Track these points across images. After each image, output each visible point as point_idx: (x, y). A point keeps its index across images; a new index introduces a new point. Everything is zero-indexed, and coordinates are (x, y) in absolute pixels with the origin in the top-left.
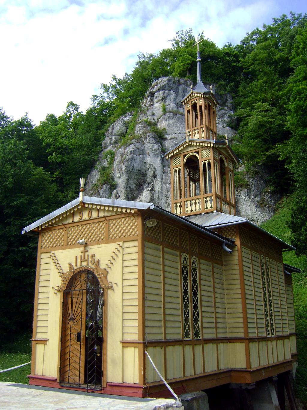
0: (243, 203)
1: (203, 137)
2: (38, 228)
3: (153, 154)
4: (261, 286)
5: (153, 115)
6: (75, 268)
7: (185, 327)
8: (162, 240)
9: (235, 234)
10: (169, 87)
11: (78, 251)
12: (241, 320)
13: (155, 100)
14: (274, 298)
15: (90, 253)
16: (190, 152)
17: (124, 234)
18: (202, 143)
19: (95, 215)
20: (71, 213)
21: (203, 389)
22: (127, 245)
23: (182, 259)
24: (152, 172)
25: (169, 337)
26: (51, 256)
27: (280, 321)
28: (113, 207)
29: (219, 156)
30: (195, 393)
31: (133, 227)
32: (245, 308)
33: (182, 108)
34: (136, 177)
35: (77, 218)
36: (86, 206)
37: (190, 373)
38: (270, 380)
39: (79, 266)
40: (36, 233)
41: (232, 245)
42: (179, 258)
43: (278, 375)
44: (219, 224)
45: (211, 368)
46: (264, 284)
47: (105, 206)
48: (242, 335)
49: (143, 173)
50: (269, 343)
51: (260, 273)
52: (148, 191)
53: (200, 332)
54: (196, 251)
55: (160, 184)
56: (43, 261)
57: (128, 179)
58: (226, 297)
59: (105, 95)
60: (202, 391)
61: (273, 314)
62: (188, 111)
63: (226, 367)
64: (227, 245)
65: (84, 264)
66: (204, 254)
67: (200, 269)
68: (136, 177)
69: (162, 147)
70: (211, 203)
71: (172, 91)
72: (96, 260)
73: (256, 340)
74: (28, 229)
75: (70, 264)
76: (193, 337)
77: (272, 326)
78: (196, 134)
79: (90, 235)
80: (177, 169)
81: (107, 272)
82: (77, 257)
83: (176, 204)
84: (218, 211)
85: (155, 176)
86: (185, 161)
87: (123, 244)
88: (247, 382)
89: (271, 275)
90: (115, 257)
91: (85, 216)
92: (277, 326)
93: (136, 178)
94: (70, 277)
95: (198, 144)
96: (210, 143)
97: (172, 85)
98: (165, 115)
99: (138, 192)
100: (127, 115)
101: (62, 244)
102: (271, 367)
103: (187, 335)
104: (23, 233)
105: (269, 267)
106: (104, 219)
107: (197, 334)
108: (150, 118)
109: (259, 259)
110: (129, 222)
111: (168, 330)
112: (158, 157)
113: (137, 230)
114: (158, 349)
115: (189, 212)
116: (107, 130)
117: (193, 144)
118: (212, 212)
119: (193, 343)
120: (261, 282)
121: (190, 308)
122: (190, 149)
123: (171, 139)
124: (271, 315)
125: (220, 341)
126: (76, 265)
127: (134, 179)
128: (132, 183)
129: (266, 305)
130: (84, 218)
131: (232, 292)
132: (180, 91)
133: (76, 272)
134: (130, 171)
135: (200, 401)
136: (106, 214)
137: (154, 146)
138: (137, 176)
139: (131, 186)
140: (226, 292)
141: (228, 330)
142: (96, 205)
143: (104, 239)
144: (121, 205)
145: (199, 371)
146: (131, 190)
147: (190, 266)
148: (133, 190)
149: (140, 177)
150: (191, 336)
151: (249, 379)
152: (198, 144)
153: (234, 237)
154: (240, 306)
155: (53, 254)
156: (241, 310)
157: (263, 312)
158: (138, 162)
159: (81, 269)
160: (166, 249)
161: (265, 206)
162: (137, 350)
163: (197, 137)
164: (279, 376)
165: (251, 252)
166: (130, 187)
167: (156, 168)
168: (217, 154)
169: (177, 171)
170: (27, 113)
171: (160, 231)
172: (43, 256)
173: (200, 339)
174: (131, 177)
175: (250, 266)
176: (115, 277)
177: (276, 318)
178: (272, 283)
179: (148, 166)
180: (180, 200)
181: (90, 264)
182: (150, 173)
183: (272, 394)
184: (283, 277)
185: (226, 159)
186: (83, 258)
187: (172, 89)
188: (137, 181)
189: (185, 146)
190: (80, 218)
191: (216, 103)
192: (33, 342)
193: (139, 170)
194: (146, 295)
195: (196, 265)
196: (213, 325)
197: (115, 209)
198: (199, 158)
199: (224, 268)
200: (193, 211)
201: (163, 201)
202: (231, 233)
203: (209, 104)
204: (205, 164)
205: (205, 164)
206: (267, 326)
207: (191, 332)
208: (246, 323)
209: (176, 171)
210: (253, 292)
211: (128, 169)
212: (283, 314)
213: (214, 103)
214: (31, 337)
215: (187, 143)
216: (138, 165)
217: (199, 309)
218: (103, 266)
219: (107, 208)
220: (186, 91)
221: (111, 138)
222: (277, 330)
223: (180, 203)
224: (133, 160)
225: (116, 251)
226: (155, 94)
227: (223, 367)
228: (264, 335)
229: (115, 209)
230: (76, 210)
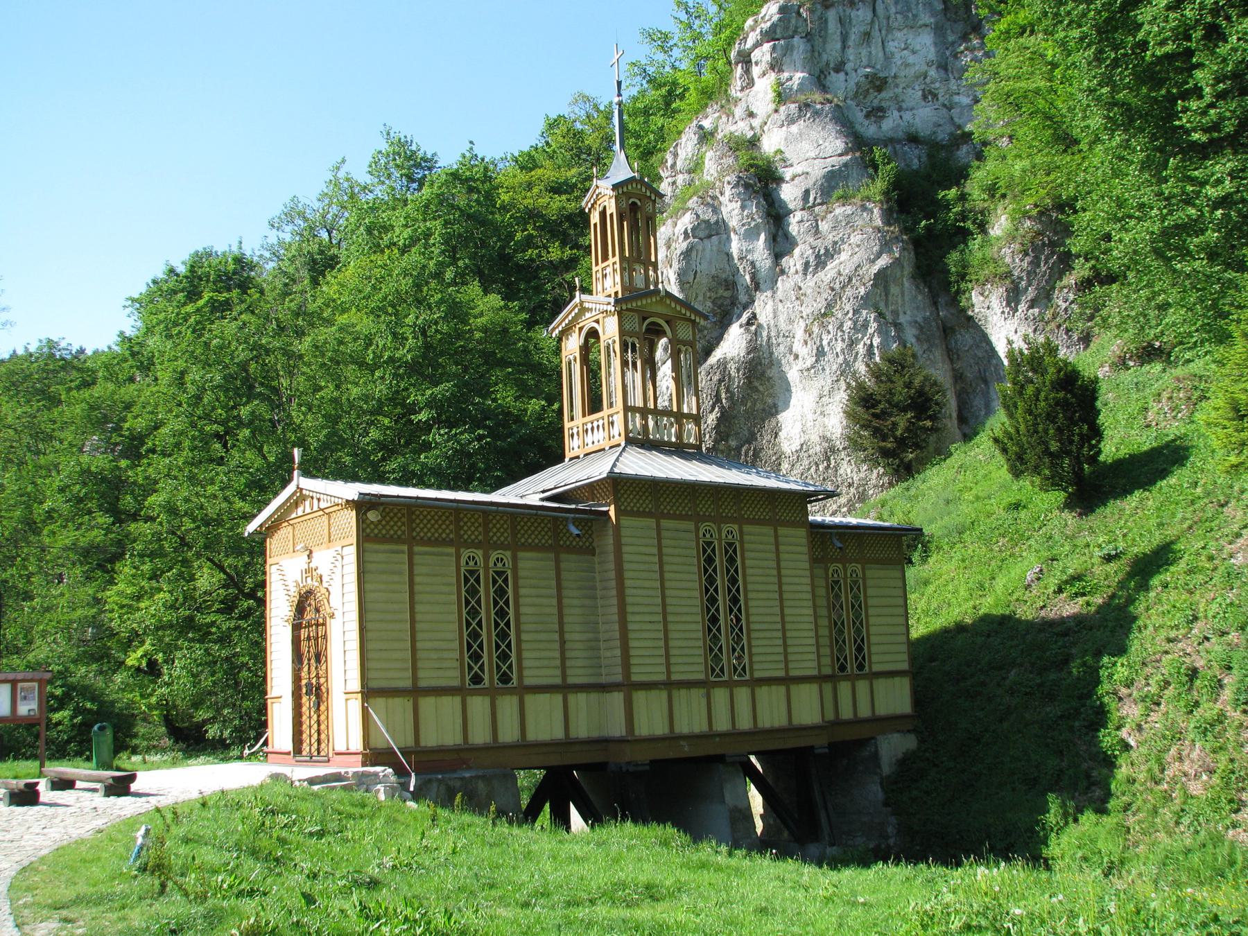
2: (261, 526)
5: (751, 115)
10: (786, 28)
13: (756, 71)
16: (587, 322)
33: (842, 76)
38: (720, 759)
48: (619, 678)
52: (741, 326)
59: (660, 57)
64: (575, 521)
67: (515, 569)
71: (796, 39)
74: (252, 527)
86: (582, 340)
97: (793, 21)
98: (776, 111)
100: (709, 110)
103: (477, 679)
107: (505, 679)
108: (741, 124)
116: (663, 162)
119: (492, 693)
122: (588, 315)
123: (793, 180)
132: (833, 26)
141: (603, 671)
161: (1059, 327)
170: (471, 142)
171: (403, 524)
176: (335, 600)
185: (667, 322)
187: (795, 32)
188: (713, 302)
192: (269, 701)
199: (596, 559)
201: (782, 348)
203: (634, 204)
207: (486, 677)
214: (266, 694)
221: (674, 183)
224: (694, 254)
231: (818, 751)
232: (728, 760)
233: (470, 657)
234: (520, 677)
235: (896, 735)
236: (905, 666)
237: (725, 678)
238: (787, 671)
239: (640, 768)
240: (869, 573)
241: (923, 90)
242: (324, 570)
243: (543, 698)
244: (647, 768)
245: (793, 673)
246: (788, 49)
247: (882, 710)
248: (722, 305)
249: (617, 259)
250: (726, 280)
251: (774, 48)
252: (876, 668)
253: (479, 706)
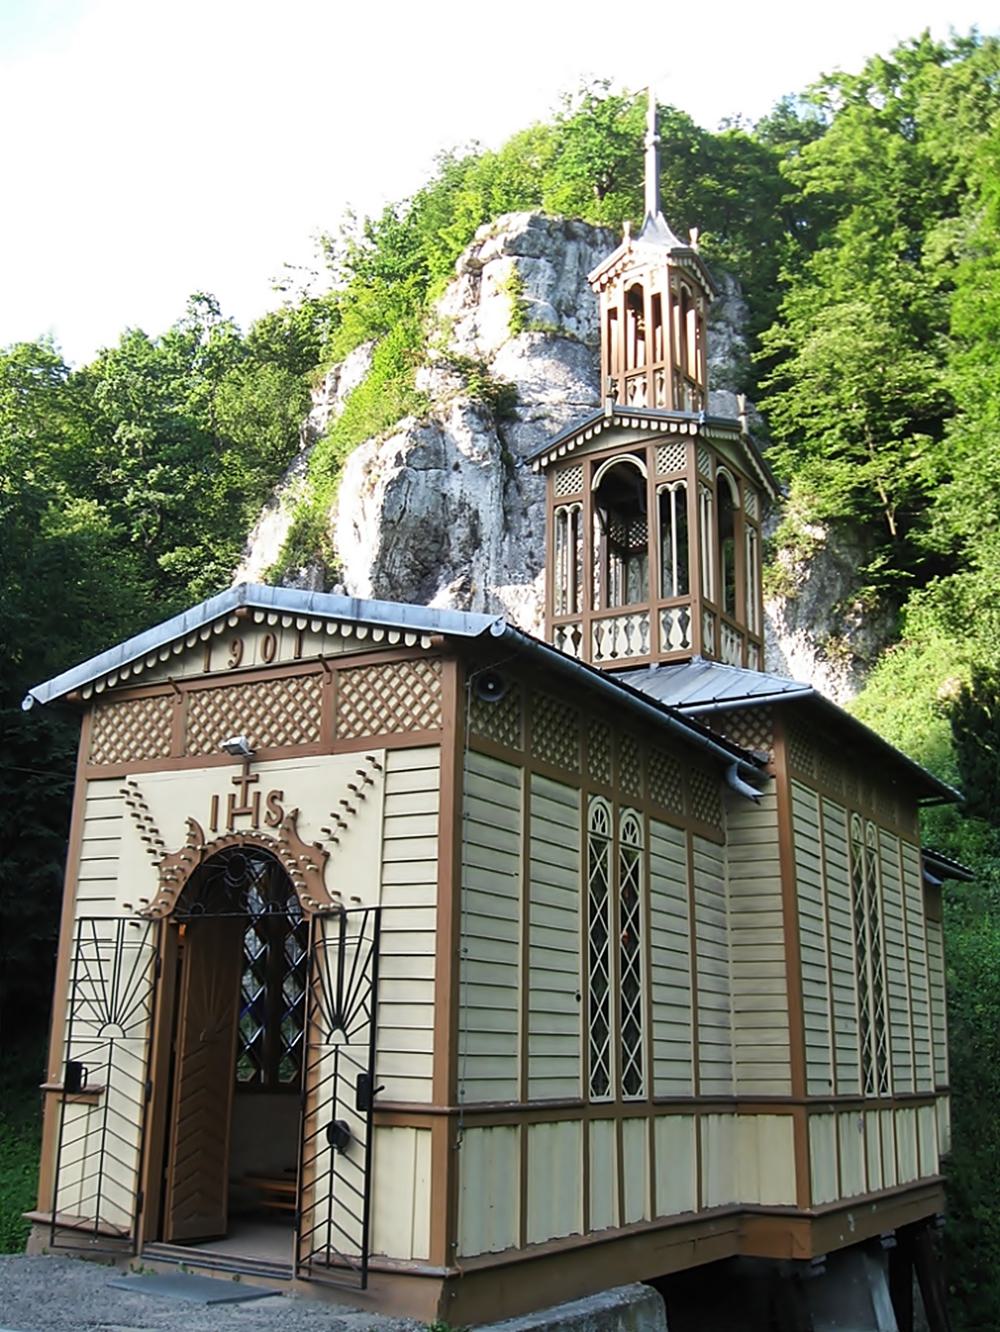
0: (770, 643)
1: (661, 404)
2: (81, 689)
3: (471, 467)
4: (850, 921)
6: (210, 837)
7: (595, 1058)
8: (522, 750)
9: (770, 738)
10: (533, 245)
11: (221, 779)
12: (784, 1037)
13: (486, 287)
14: (891, 963)
15: (265, 787)
16: (617, 448)
17: (391, 723)
18: (659, 422)
19: (286, 651)
20: (200, 643)
21: (645, 1278)
22: (398, 760)
23: (591, 815)
24: (467, 530)
25: (539, 1092)
26: (123, 791)
27: (908, 1046)
28: (355, 624)
29: (714, 473)
30: (624, 1289)
31: (426, 699)
32: (796, 996)
34: (411, 543)
35: (221, 661)
36: (259, 618)
37: (605, 1220)
38: (870, 1246)
39: (223, 831)
40: (73, 710)
41: (758, 775)
42: (578, 814)
43: (897, 1230)
44: (714, 701)
45: (678, 1202)
46: (859, 915)
47: (325, 620)
48: (784, 1090)
49: (436, 530)
50: (872, 1118)
51: (848, 874)
52: (452, 590)
53: (644, 1077)
54: (635, 790)
55: (493, 568)
56: (93, 809)
57: (384, 549)
58: (731, 953)
60: (644, 1283)
61: (886, 1020)
62: (612, 314)
63: (724, 1201)
64: (744, 775)
65: (243, 824)
66: (663, 802)
68: (411, 543)
69: (504, 444)
70: (684, 631)
71: (542, 261)
72: (288, 812)
73: (832, 1108)
74: (45, 692)
75: (192, 824)
76: (619, 1093)
77: (882, 1059)
78: (639, 391)
79: (266, 721)
80: (568, 509)
81: (327, 855)
82: (216, 798)
83: (561, 629)
84: (705, 656)
85: (475, 541)
86: (596, 484)
87: (386, 758)
88: (797, 1255)
89: (882, 886)
90: (354, 803)
91: (253, 653)
92: (899, 1059)
93: (412, 547)
94: (190, 870)
95: (644, 424)
96: (688, 421)
97: (543, 240)
99: (416, 593)
101: (166, 750)
102: (877, 1201)
103: (600, 1083)
104: (26, 705)
105: (876, 857)
106: (319, 667)
107: (631, 1082)
109: (846, 829)
110: (411, 680)
111: (536, 1068)
112: (487, 478)
113: (438, 711)
114: (499, 1132)
115: (607, 657)
117: (626, 423)
118: (688, 661)
120: (850, 907)
121: (610, 989)
124: (880, 1023)
125: (707, 1109)
126: (215, 830)
127: (406, 549)
128: (397, 564)
129: (863, 985)
130: (246, 663)
131: (752, 937)
132: (570, 262)
133: (212, 852)
134: (392, 521)
136: (329, 650)
137: (477, 440)
138: (414, 538)
139: (395, 571)
140: (731, 937)
141: (735, 1071)
142: (295, 616)
143: (318, 739)
144: (384, 619)
145: (638, 1212)
146: (393, 588)
147: (616, 842)
148: (401, 586)
149: (427, 542)
150: (612, 1086)
151: (805, 1246)
152: (644, 424)
153: (764, 747)
154: (781, 986)
155: (131, 783)
156: (782, 1003)
157: (855, 1012)
158: (421, 491)
159: (231, 842)
160: (534, 779)
162: (426, 1139)
163: (639, 401)
164: (903, 1233)
165: (821, 801)
166: (389, 575)
167: (480, 514)
168: (709, 462)
169: (569, 516)
172: (95, 790)
173: (641, 1098)
174: (397, 544)
175: (817, 849)
177: (896, 1032)
178: (884, 914)
179: (453, 507)
180: (576, 618)
181: (262, 823)
182: (459, 532)
183: (876, 1296)
184: (919, 894)
185: (737, 479)
186: (238, 804)
187: (542, 252)
189: (598, 430)
190: (234, 659)
191: (708, 290)
193: (423, 521)
194: (464, 943)
195: (634, 841)
196: (688, 1052)
197: (361, 633)
198: (645, 474)
200: (618, 657)
202: (757, 733)
203: (684, 289)
204: (665, 495)
205: (665, 495)
206: (867, 1059)
207: (612, 1077)
208: (798, 1046)
209: (564, 514)
210: (825, 940)
211: (389, 516)
212: (917, 1020)
213: (703, 289)
215: (605, 419)
216: (422, 502)
217: (642, 993)
218: (309, 834)
219: (331, 629)
220: (590, 263)
222: (899, 1074)
223: (575, 627)
224: (405, 485)
225: (359, 781)
226: (485, 269)
227: (714, 1199)
228: (857, 1089)
229: (361, 633)
230: (218, 630)
237: (874, 1094)
244: (822, 1269)
246: (533, 271)
248: (425, 560)
249: (667, 364)
250: (436, 530)
251: (517, 264)
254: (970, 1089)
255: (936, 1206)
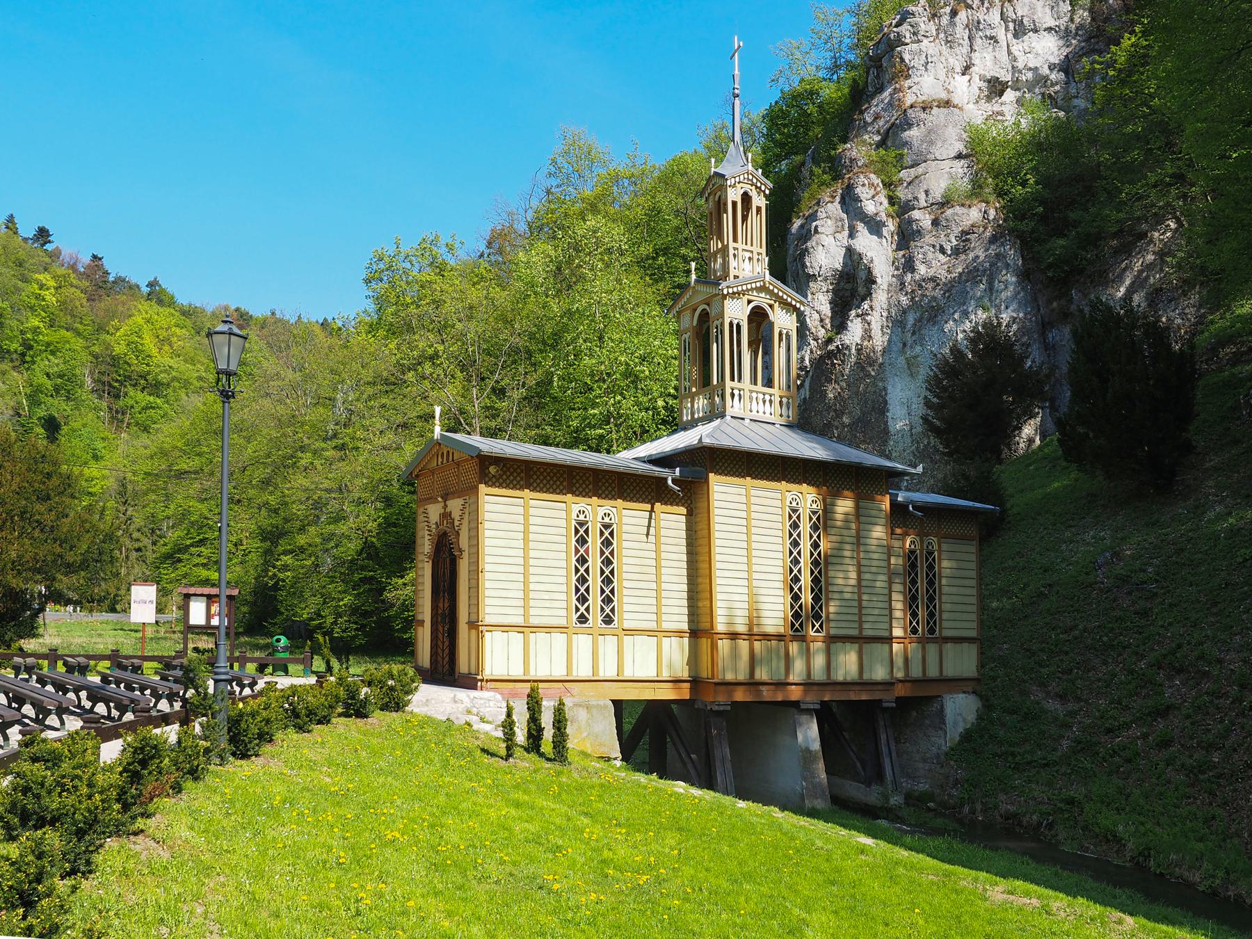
15: (448, 510)
25: (534, 621)
33: (967, 77)
67: (620, 524)
103: (583, 619)
107: (608, 620)
119: (595, 635)
132: (961, 32)
135: (594, 711)
231: (885, 705)
232: (803, 706)
233: (578, 600)
234: (621, 620)
235: (962, 695)
236: (973, 634)
238: (861, 631)
239: (722, 708)
240: (944, 547)
241: (1043, 94)
242: (456, 515)
243: (639, 639)
245: (865, 633)
247: (949, 672)
252: (946, 633)
253: (583, 643)
254: (984, 643)
255: (888, 699)
